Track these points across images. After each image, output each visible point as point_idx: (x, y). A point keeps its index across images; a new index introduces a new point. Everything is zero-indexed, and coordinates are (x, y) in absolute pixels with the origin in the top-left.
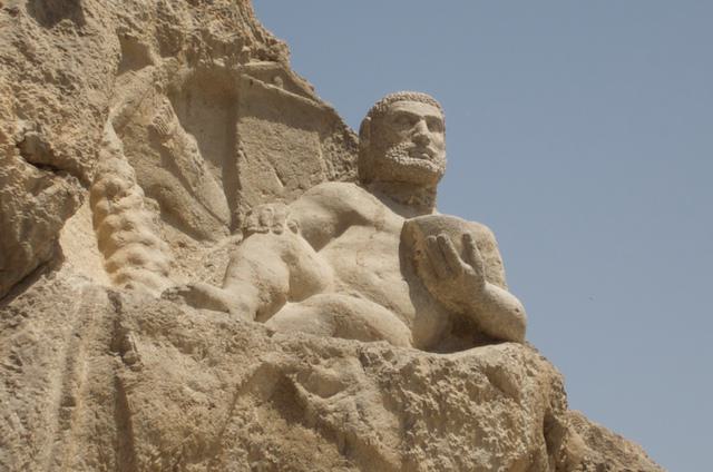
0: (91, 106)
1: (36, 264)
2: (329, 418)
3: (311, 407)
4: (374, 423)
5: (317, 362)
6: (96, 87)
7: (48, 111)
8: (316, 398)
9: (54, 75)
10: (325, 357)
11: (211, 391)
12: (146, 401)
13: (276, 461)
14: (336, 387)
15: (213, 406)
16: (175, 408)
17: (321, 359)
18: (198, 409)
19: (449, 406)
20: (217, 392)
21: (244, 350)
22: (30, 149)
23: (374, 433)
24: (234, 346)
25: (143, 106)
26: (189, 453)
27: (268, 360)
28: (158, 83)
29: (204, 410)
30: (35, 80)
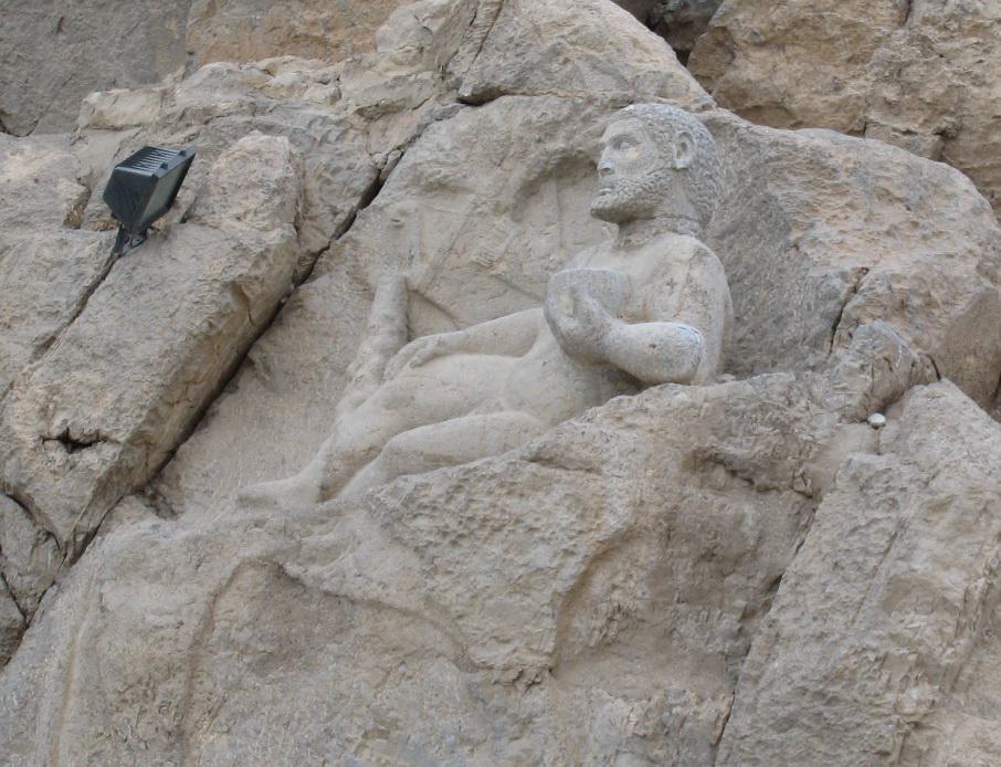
0: (139, 362)
1: (80, 538)
2: (326, 586)
3: (309, 582)
4: (374, 575)
5: (309, 533)
6: (149, 338)
7: (85, 394)
8: (314, 569)
9: (100, 351)
10: (322, 522)
11: (179, 611)
12: (110, 643)
13: (270, 648)
14: (332, 552)
15: (181, 623)
16: (138, 641)
17: (317, 529)
18: (162, 632)
19: (470, 519)
20: (185, 611)
21: (219, 554)
22: (75, 435)
23: (374, 585)
24: (208, 554)
25: (459, 246)
26: (158, 675)
27: (247, 554)
28: (479, 210)
29: (170, 632)
30: (79, 367)
